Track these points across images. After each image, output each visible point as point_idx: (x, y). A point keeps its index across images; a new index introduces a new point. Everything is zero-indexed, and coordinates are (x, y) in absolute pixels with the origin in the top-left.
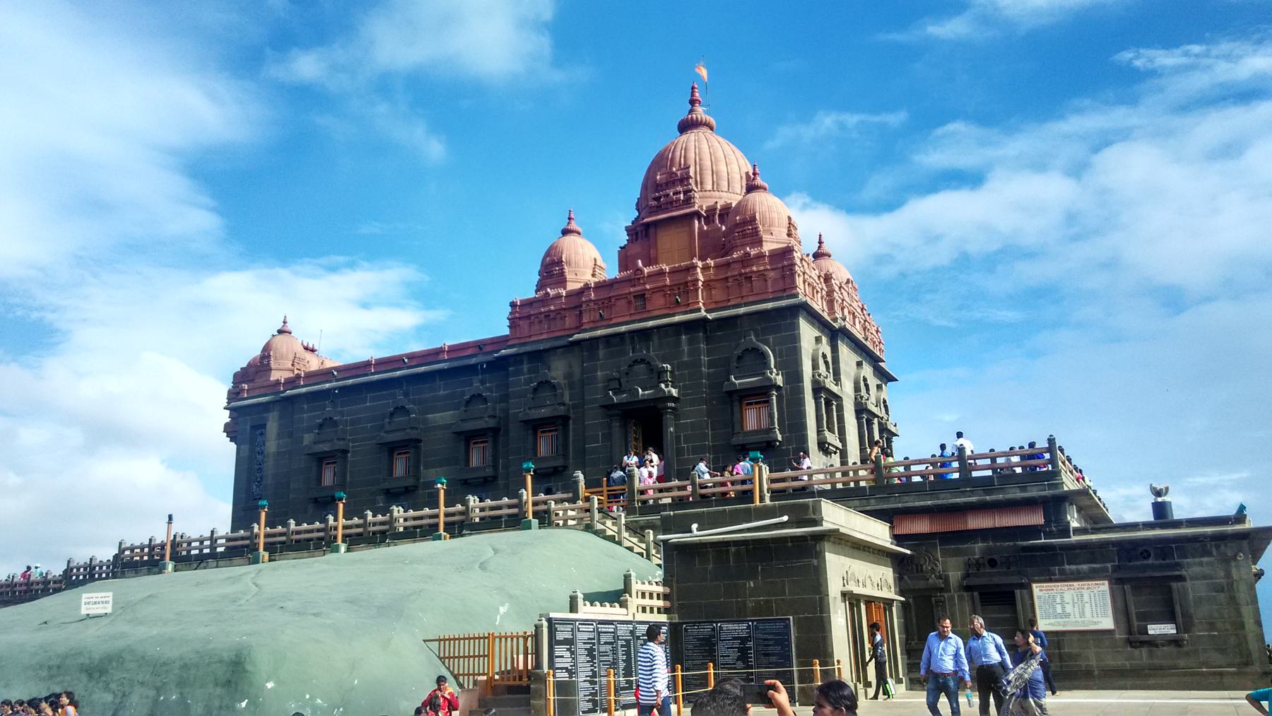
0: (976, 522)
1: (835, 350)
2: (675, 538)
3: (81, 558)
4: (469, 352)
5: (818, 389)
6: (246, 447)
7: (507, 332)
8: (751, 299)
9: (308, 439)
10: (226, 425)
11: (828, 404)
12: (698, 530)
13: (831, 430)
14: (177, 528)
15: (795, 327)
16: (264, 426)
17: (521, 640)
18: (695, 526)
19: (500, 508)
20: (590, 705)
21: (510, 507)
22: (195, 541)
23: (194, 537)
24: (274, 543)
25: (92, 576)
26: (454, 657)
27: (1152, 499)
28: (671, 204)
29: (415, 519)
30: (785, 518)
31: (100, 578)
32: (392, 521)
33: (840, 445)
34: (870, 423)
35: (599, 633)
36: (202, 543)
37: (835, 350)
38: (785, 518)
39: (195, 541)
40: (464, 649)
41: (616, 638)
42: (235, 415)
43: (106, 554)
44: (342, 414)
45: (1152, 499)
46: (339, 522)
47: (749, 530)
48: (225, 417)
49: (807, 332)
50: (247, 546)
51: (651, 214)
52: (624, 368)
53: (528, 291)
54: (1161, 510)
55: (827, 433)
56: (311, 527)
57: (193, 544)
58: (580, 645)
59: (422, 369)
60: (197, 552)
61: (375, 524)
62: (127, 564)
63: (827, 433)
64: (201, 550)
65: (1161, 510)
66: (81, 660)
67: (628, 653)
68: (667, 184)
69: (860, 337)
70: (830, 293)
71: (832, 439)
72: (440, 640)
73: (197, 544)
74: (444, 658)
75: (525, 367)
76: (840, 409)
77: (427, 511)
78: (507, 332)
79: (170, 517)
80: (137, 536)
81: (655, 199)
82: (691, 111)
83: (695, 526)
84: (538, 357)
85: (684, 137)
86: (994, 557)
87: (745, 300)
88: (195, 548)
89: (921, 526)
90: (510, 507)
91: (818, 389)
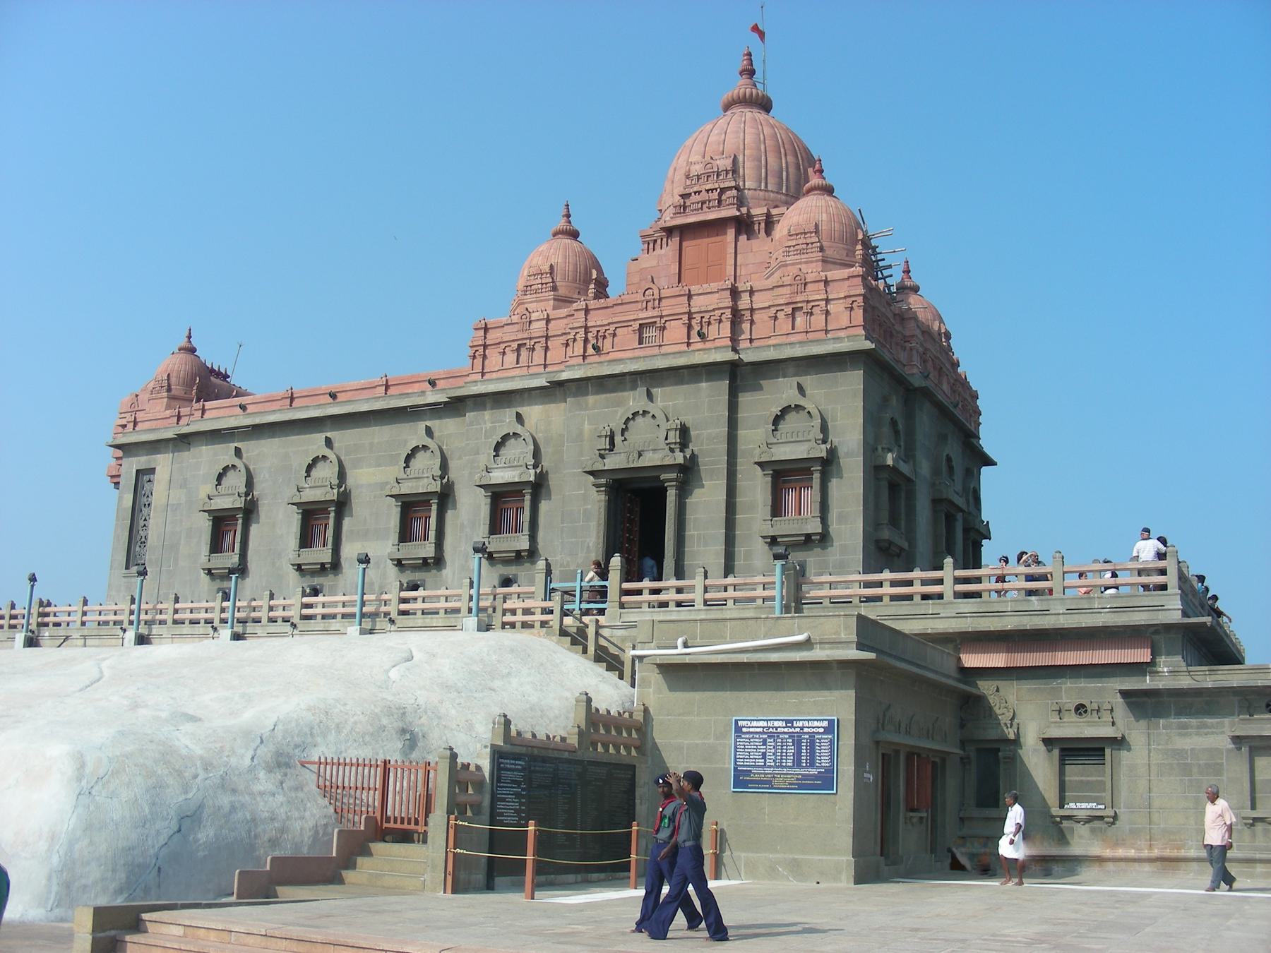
16: (152, 471)
68: (699, 177)
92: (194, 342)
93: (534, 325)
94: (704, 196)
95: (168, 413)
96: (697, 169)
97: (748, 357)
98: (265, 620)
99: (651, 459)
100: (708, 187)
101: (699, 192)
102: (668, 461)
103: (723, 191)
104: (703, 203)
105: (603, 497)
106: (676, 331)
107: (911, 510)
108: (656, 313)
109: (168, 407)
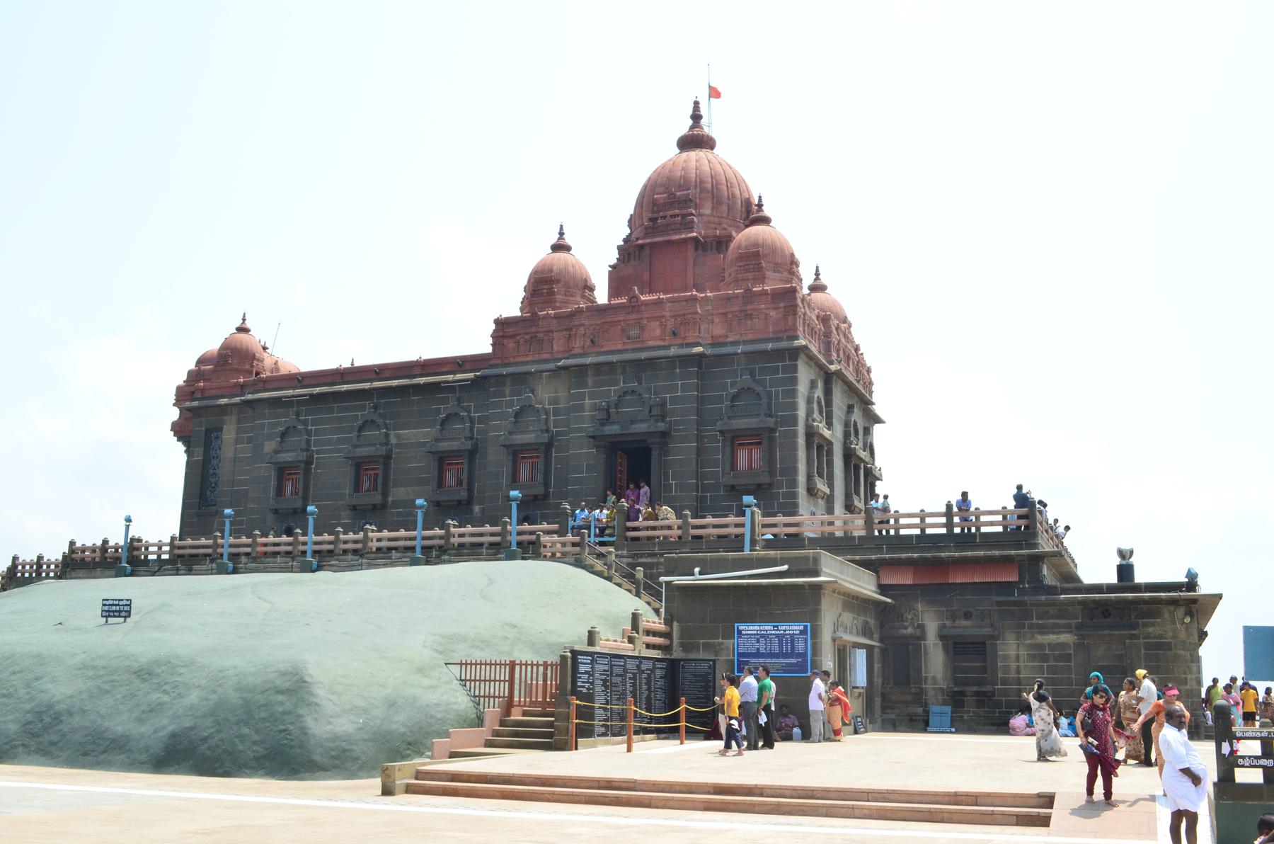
0: (959, 579)
1: (828, 392)
2: (678, 580)
3: (28, 556)
5: (811, 434)
6: (199, 451)
7: (489, 350)
8: (750, 337)
9: (269, 446)
11: (820, 447)
12: (700, 573)
13: (820, 475)
14: (134, 532)
15: (794, 369)
17: (541, 668)
18: (697, 570)
19: (481, 535)
20: (603, 730)
21: (492, 535)
22: (153, 545)
23: (151, 541)
24: (238, 555)
25: (39, 574)
26: (475, 680)
27: (1118, 561)
28: (667, 229)
29: (390, 540)
30: (785, 567)
31: (48, 577)
32: (366, 540)
33: (828, 491)
34: (857, 468)
35: (612, 666)
36: (160, 548)
37: (828, 392)
38: (785, 567)
39: (153, 545)
40: (485, 672)
41: (625, 671)
42: (189, 414)
43: (55, 553)
44: (305, 423)
45: (1118, 561)
46: (310, 540)
47: (751, 577)
48: (175, 414)
49: (804, 375)
50: (209, 555)
51: (646, 236)
52: (614, 398)
53: (513, 309)
54: (1125, 571)
55: (817, 479)
56: (277, 540)
57: (151, 549)
58: (597, 676)
59: (395, 383)
60: (155, 557)
61: (345, 542)
62: (77, 564)
63: (817, 479)
64: (159, 556)
65: (1125, 571)
66: (127, 663)
67: (634, 685)
68: (664, 204)
69: (852, 378)
70: (828, 335)
71: (822, 486)
72: (461, 664)
73: (155, 549)
74: (466, 680)
76: (830, 453)
77: (402, 533)
78: (489, 350)
79: (128, 520)
80: (89, 538)
82: (692, 128)
83: (697, 570)
84: (521, 380)
85: (684, 155)
86: (971, 610)
87: (744, 338)
88: (153, 553)
89: (906, 579)
90: (492, 535)
91: (811, 434)
94: (668, 220)
99: (641, 427)
100: (671, 213)
101: (664, 217)
103: (684, 216)
107: (830, 464)
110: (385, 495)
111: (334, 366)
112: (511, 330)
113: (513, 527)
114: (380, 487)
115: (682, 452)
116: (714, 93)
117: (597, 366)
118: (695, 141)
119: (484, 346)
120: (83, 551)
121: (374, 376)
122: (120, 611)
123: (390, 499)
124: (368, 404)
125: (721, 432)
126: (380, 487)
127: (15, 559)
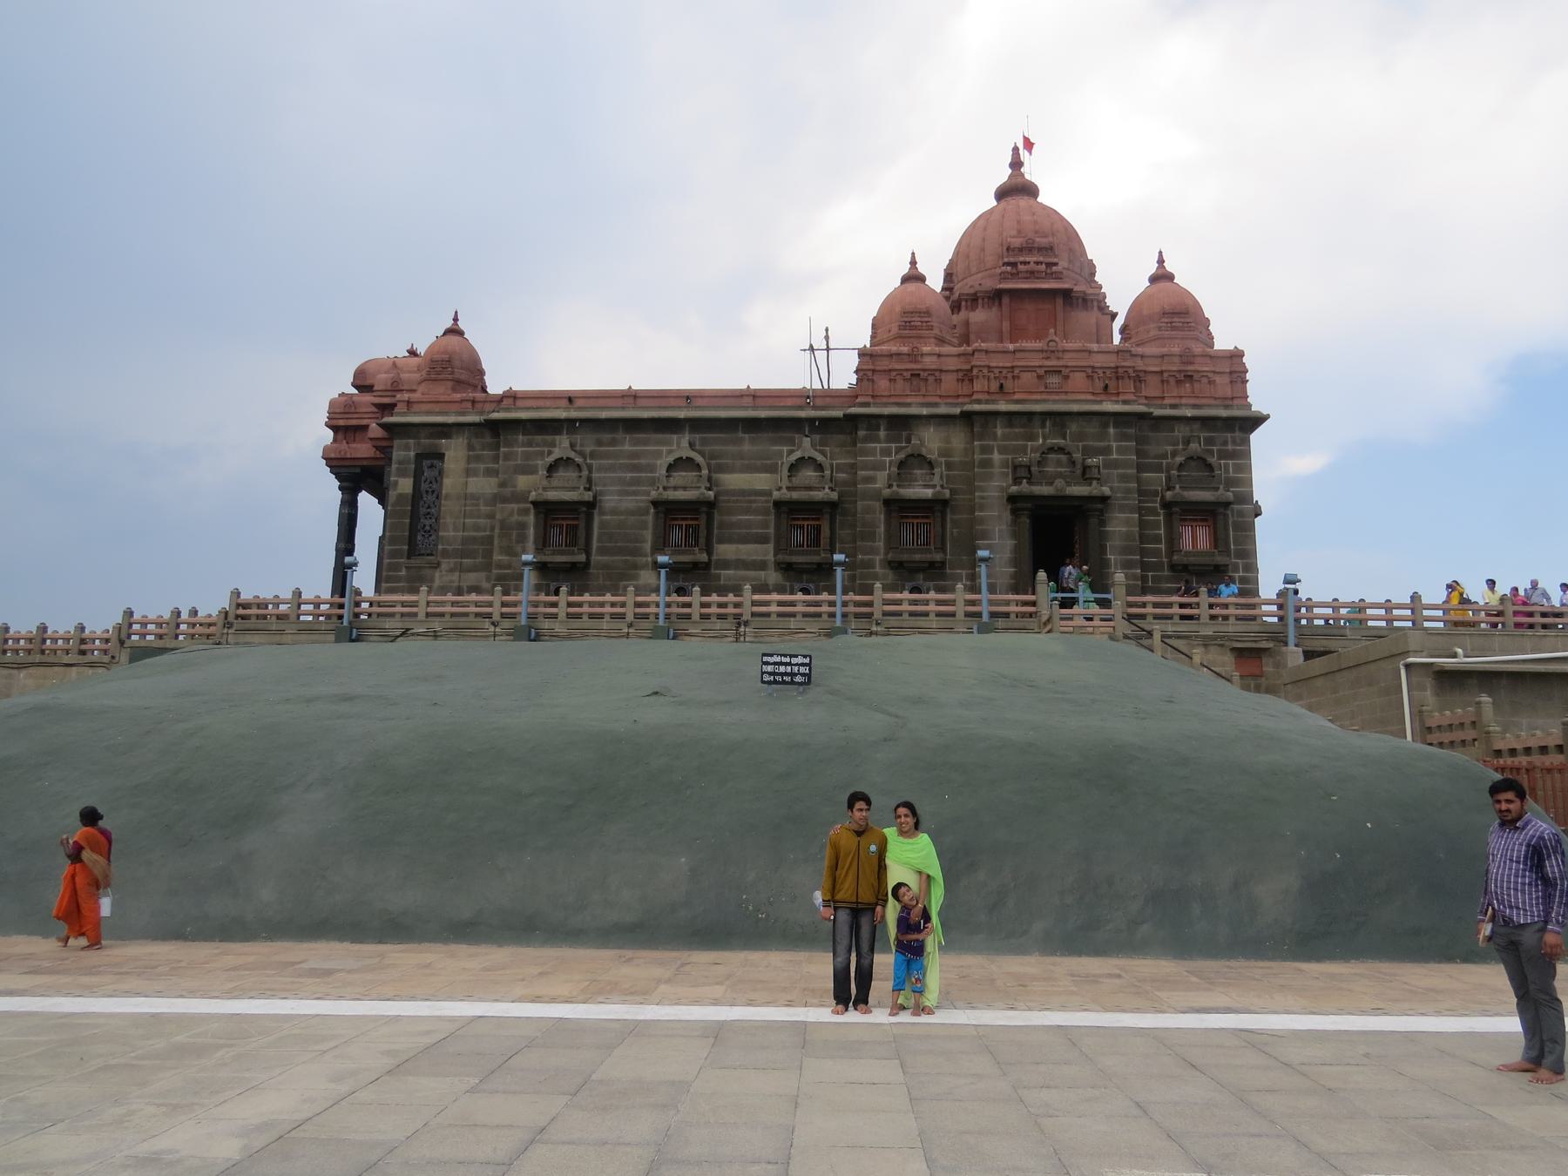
4: (789, 402)
10: (326, 449)
16: (441, 457)
43: (213, 604)
68: (1021, 250)
75: (882, 433)
81: (1008, 264)
84: (901, 424)
92: (461, 325)
93: (927, 359)
94: (1032, 266)
95: (458, 396)
96: (1017, 242)
97: (1157, 412)
98: (696, 617)
101: (1025, 263)
102: (1095, 492)
103: (1050, 265)
104: (1032, 272)
105: (1025, 520)
106: (1078, 379)
108: (1061, 363)
109: (454, 390)
110: (710, 553)
111: (621, 385)
112: (883, 364)
113: (985, 596)
114: (702, 541)
115: (1120, 525)
116: (1029, 145)
117: (1010, 415)
118: (1017, 189)
119: (844, 376)
120: (277, 605)
121: (683, 403)
122: (792, 675)
123: (714, 557)
124: (685, 439)
125: (1167, 505)
126: (702, 541)
127: (129, 613)
